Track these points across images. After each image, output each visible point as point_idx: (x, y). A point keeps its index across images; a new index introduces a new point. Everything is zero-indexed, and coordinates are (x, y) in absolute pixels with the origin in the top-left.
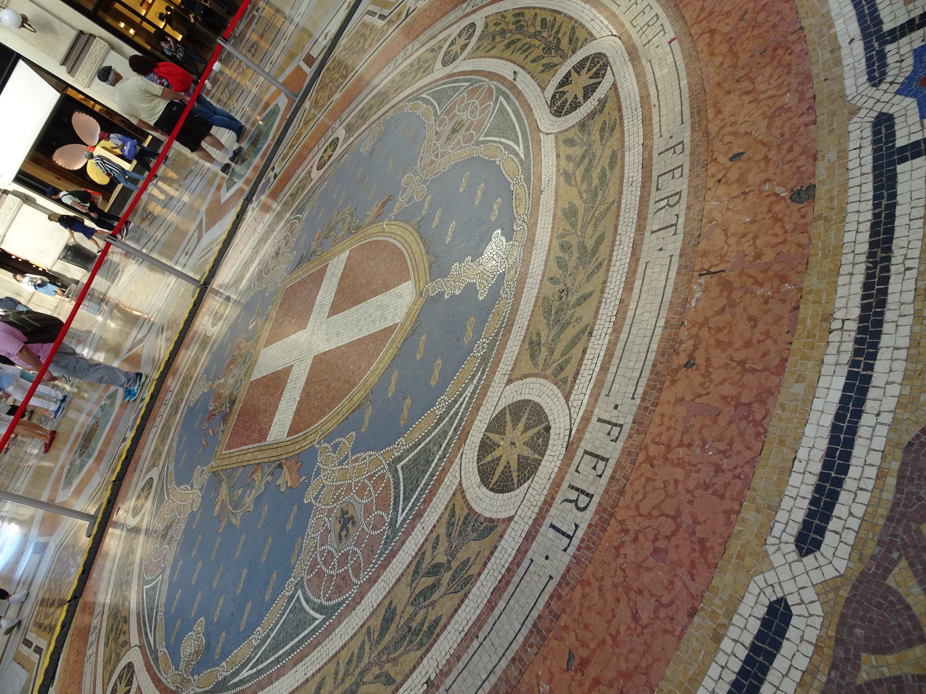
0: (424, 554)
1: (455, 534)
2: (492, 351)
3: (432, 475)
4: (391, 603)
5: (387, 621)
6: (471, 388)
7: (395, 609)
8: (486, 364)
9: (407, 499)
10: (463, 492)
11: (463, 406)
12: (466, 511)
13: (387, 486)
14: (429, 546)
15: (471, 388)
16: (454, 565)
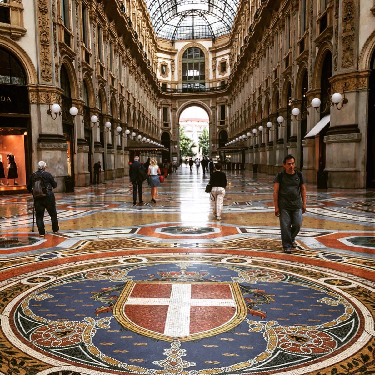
0: (32, 359)
1: (33, 368)
2: (117, 369)
3: (66, 357)
4: (18, 353)
5: (11, 353)
6: (102, 364)
7: (14, 354)
8: (111, 368)
9: (61, 351)
10: (50, 368)
11: (94, 363)
12: (40, 370)
13: (72, 343)
14: (34, 360)
15: (102, 364)
16: (20, 369)
